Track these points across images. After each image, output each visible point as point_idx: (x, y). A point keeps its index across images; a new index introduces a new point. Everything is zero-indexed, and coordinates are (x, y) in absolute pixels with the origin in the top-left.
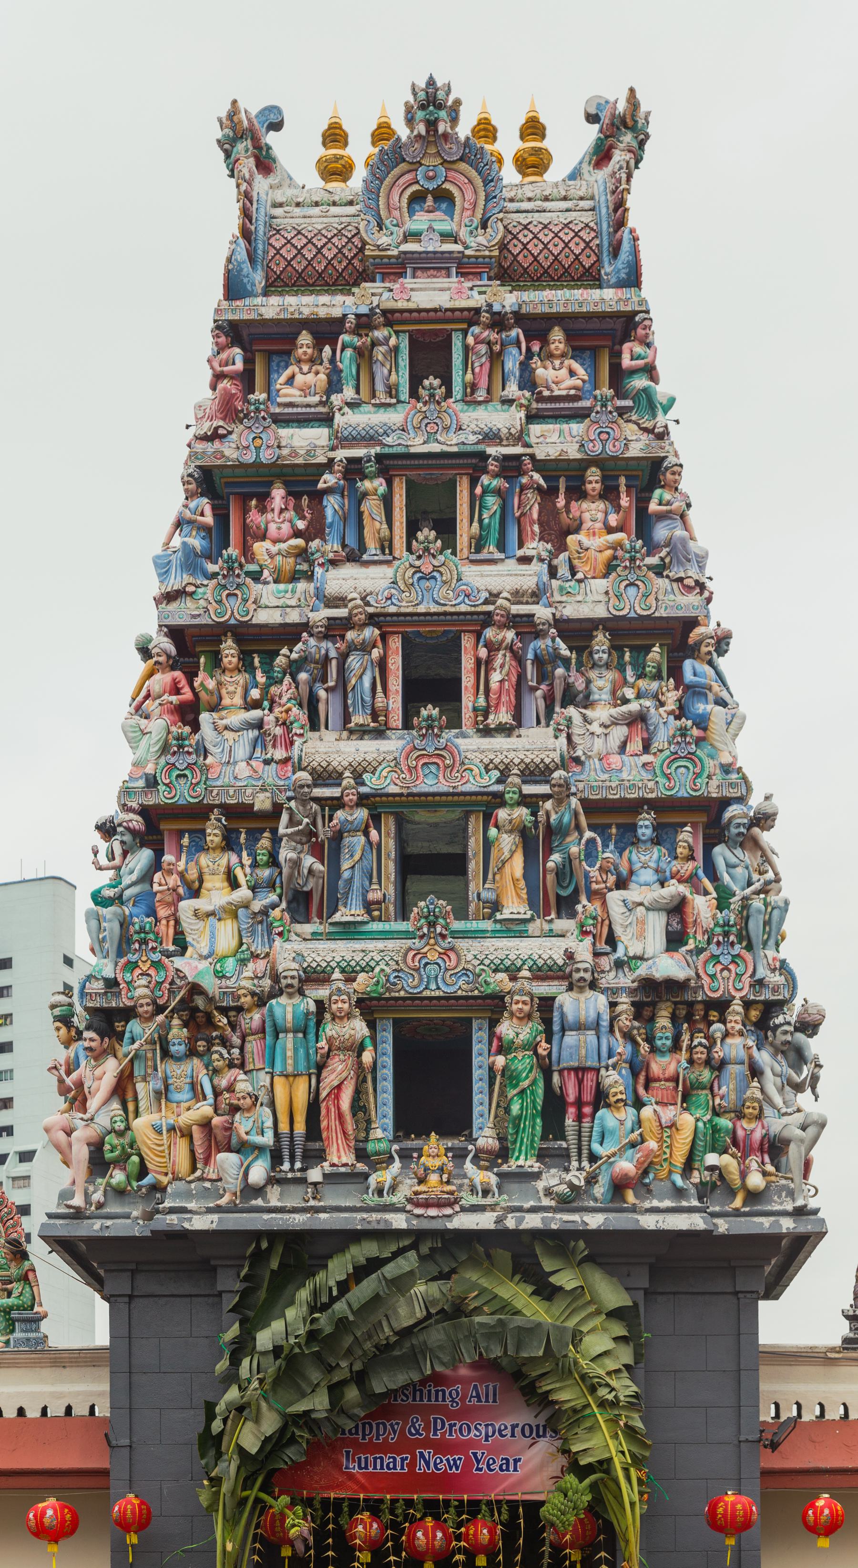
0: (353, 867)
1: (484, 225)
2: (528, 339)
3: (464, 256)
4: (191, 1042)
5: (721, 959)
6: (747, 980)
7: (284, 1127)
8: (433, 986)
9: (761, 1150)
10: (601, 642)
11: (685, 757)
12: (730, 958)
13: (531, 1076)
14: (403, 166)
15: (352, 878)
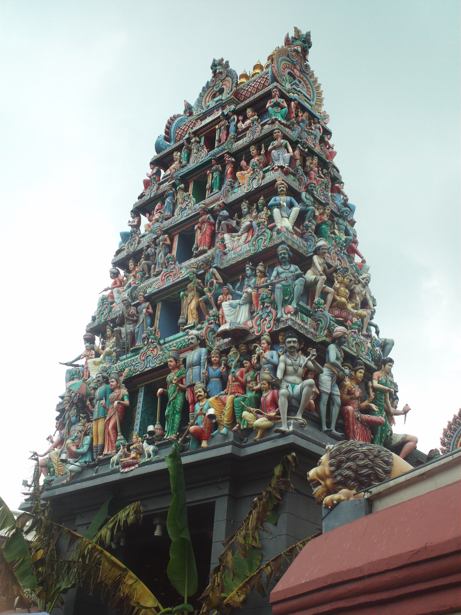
0: (139, 327)
1: (231, 90)
2: (238, 116)
3: (223, 104)
4: (78, 416)
5: (263, 317)
6: (272, 322)
7: (94, 444)
8: (148, 366)
9: (271, 405)
10: (244, 206)
11: (261, 235)
12: (266, 314)
13: (174, 395)
14: (210, 89)
15: (138, 332)
